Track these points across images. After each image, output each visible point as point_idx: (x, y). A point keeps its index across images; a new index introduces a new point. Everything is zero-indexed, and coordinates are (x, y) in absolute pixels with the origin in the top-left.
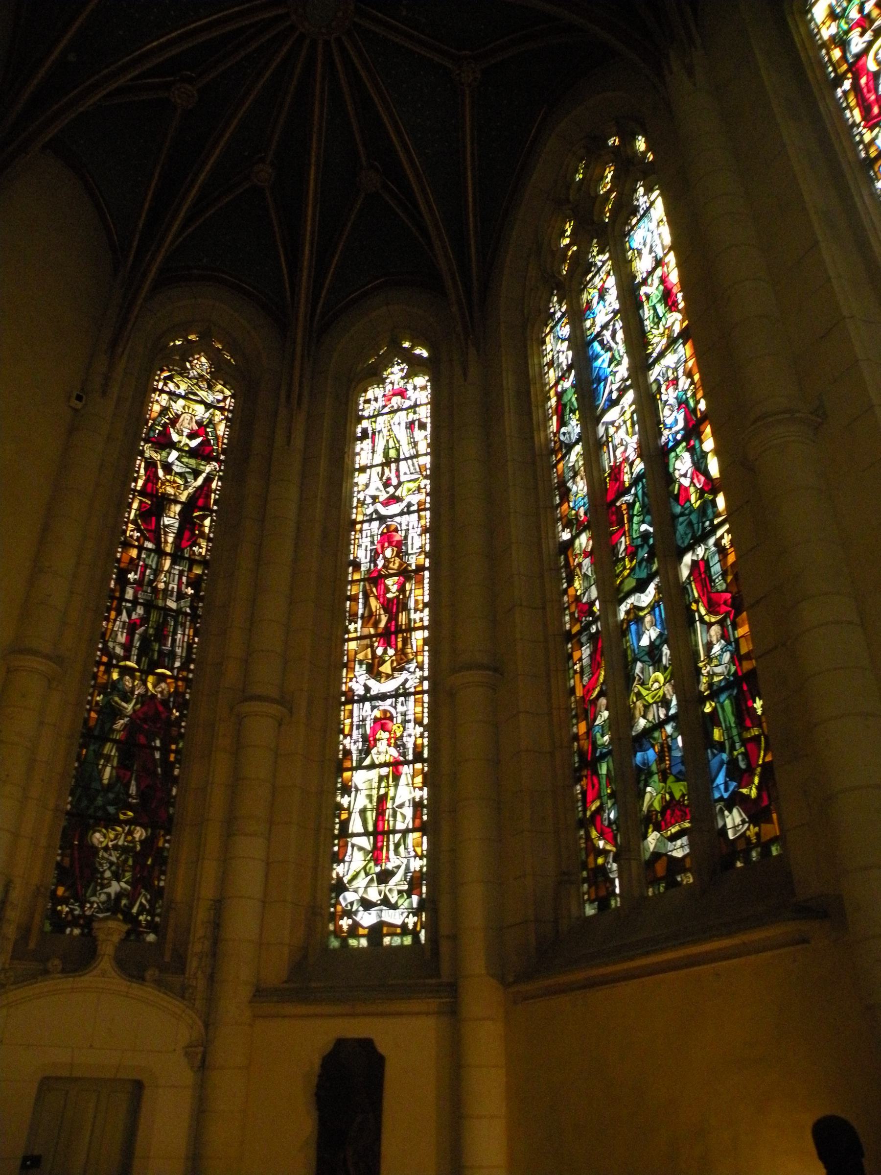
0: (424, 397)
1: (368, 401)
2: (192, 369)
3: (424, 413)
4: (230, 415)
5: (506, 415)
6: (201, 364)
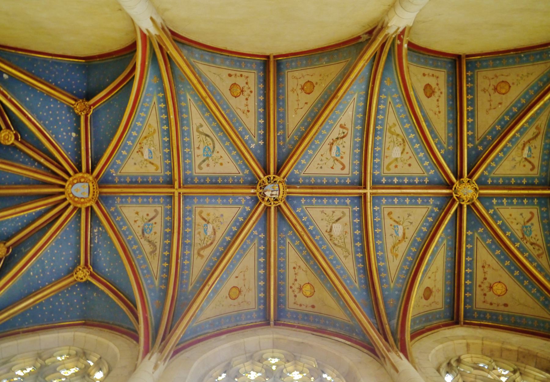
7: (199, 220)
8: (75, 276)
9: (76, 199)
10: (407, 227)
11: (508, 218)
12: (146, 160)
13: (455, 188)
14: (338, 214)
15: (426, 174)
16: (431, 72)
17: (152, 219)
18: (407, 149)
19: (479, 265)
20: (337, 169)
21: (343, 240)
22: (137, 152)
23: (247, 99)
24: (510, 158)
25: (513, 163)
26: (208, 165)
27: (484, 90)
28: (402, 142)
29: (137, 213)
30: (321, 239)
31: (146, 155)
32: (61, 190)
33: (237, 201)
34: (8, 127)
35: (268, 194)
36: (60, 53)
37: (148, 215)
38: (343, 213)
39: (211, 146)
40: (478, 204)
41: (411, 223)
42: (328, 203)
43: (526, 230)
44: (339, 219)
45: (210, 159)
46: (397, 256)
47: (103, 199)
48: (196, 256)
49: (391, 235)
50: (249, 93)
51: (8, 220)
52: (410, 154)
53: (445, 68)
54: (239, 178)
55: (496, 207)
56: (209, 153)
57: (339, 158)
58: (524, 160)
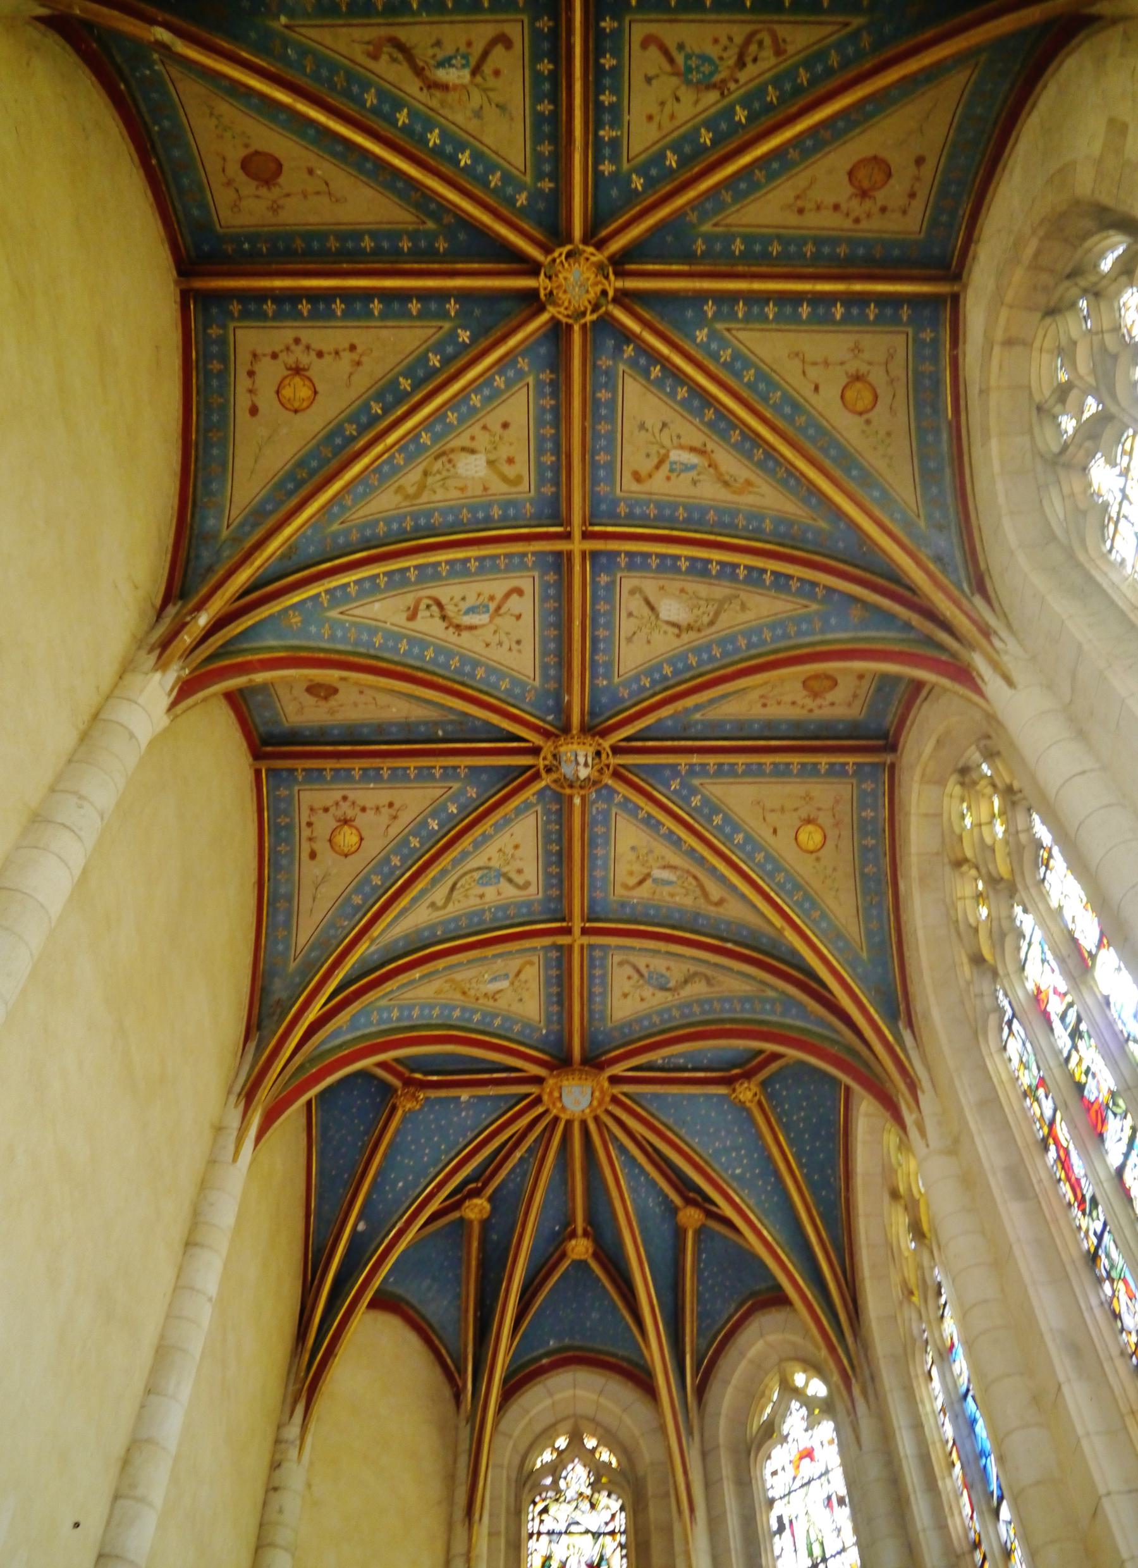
0: (830, 1456)
1: (774, 1473)
2: (568, 1488)
3: (839, 1486)
4: (623, 1539)
5: (912, 1498)
6: (577, 1477)
7: (644, 892)
8: (748, 1104)
9: (595, 1103)
10: (675, 438)
11: (660, 126)
12: (512, 983)
13: (568, 316)
14: (635, 604)
15: (531, 380)
16: (243, 382)
17: (638, 971)
18: (463, 440)
19: (793, 219)
20: (524, 605)
21: (702, 603)
22: (495, 1000)
23: (363, 809)
24: (473, 126)
25: (491, 113)
26: (520, 871)
27: (275, 208)
28: (444, 459)
29: (625, 995)
30: (697, 651)
31: (504, 984)
32: (576, 1127)
33: (600, 817)
34: (457, 1206)
35: (583, 773)
36: (304, 1136)
37: (629, 978)
38: (632, 592)
39: (477, 875)
40: (615, 246)
41: (664, 425)
42: (609, 626)
43: (696, 74)
44: (648, 603)
45: (505, 870)
46: (748, 483)
47: (594, 1062)
48: (721, 910)
49: (695, 483)
50: (348, 803)
51: (634, 1201)
52: (476, 430)
53: (224, 327)
54: (547, 812)
55: (625, 166)
56: (493, 874)
57: (492, 606)
58: (478, 79)
